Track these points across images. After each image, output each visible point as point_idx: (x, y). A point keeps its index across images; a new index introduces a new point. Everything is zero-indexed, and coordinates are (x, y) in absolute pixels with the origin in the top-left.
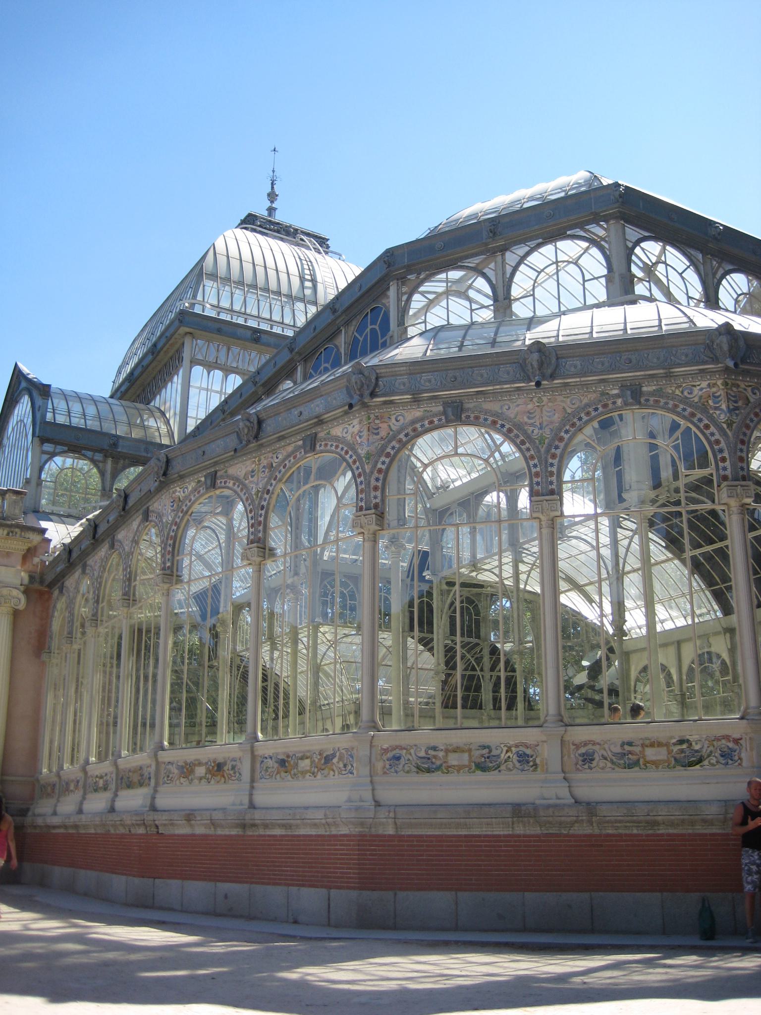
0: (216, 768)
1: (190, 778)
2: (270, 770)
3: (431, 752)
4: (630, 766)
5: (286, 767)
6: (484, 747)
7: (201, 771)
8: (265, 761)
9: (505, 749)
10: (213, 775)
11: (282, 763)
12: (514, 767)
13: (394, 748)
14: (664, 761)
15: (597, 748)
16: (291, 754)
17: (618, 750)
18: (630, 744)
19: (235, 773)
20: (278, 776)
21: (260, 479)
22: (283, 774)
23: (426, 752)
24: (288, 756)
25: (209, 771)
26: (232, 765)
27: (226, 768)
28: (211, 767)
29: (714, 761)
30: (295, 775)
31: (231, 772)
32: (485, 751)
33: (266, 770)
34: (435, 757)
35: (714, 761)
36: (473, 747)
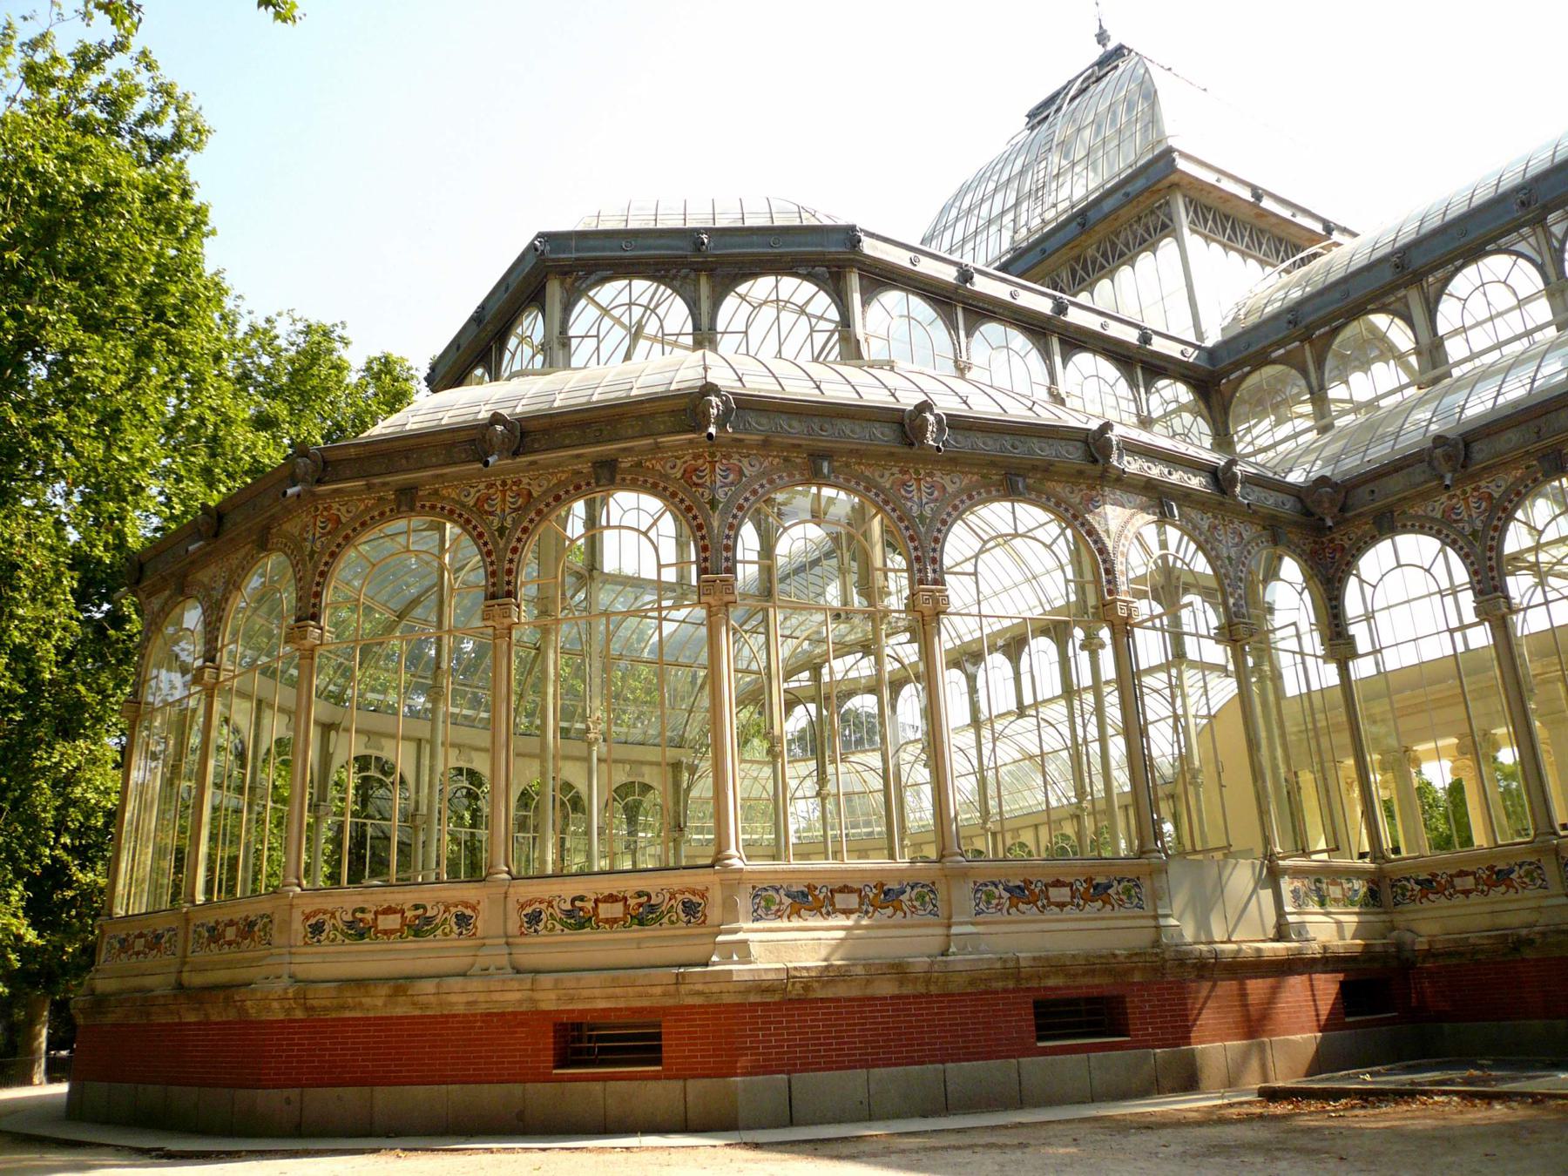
3: (359, 915)
4: (582, 926)
6: (416, 907)
9: (442, 908)
12: (451, 931)
13: (315, 913)
14: (621, 919)
15: (543, 906)
17: (568, 906)
18: (581, 898)
23: (353, 914)
29: (674, 918)
32: (420, 911)
34: (361, 920)
35: (674, 918)
36: (405, 907)
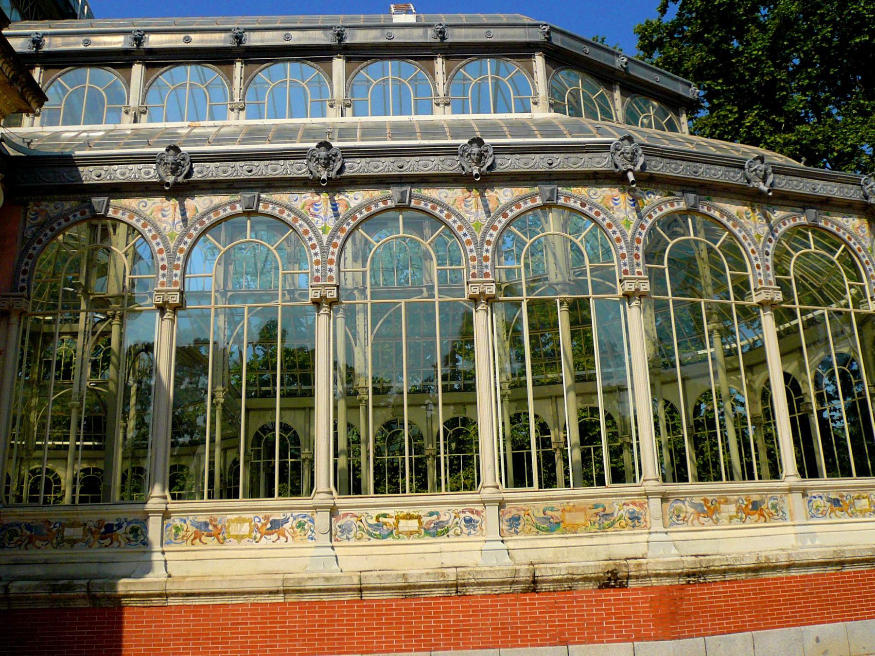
0: (750, 507)
1: (714, 517)
2: (821, 509)
5: (841, 506)
7: (732, 509)
8: (814, 500)
10: (748, 514)
11: (836, 502)
16: (845, 494)
19: (777, 512)
20: (833, 515)
21: (758, 225)
22: (837, 512)
24: (842, 496)
25: (739, 510)
26: (772, 504)
27: (764, 507)
28: (744, 506)
30: (853, 513)
31: (773, 511)
33: (818, 510)
